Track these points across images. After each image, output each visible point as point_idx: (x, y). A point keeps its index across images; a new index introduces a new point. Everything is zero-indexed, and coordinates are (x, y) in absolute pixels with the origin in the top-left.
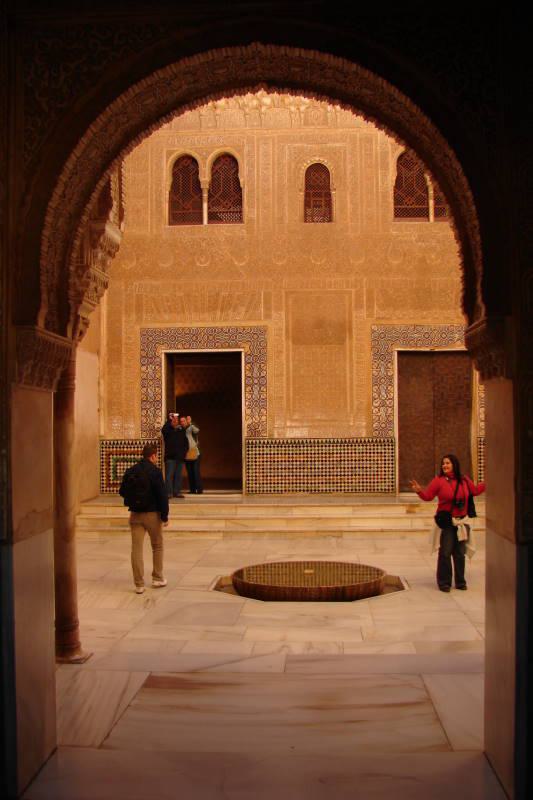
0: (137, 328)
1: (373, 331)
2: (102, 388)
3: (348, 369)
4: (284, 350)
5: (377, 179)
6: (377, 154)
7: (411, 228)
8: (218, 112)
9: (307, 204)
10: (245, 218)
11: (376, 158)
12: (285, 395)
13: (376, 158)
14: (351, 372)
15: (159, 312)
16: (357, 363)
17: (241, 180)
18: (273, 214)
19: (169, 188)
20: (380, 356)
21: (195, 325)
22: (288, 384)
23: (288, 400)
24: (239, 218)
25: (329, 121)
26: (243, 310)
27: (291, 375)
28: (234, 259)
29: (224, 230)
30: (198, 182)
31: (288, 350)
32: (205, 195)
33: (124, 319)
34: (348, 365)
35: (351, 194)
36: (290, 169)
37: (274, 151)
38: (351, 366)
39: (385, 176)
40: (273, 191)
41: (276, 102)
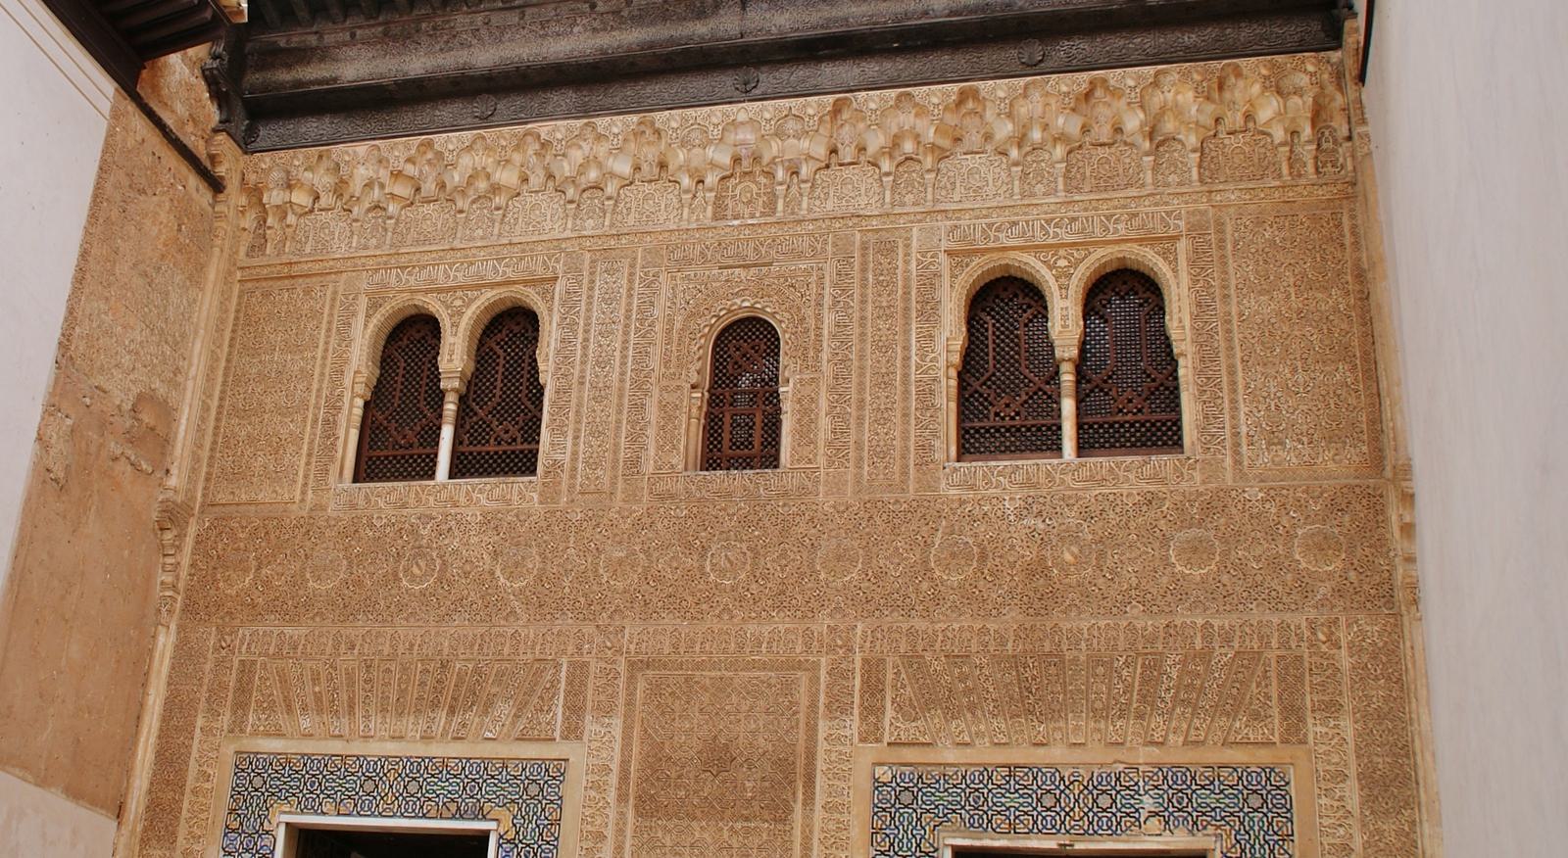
1: (878, 784)
5: (907, 348)
6: (907, 280)
11: (906, 293)
13: (906, 293)
17: (541, 367)
18: (616, 445)
19: (360, 389)
24: (524, 463)
25: (780, 206)
28: (498, 573)
29: (485, 492)
30: (436, 377)
32: (450, 407)
35: (832, 389)
36: (669, 331)
37: (630, 289)
40: (621, 389)
41: (645, 167)
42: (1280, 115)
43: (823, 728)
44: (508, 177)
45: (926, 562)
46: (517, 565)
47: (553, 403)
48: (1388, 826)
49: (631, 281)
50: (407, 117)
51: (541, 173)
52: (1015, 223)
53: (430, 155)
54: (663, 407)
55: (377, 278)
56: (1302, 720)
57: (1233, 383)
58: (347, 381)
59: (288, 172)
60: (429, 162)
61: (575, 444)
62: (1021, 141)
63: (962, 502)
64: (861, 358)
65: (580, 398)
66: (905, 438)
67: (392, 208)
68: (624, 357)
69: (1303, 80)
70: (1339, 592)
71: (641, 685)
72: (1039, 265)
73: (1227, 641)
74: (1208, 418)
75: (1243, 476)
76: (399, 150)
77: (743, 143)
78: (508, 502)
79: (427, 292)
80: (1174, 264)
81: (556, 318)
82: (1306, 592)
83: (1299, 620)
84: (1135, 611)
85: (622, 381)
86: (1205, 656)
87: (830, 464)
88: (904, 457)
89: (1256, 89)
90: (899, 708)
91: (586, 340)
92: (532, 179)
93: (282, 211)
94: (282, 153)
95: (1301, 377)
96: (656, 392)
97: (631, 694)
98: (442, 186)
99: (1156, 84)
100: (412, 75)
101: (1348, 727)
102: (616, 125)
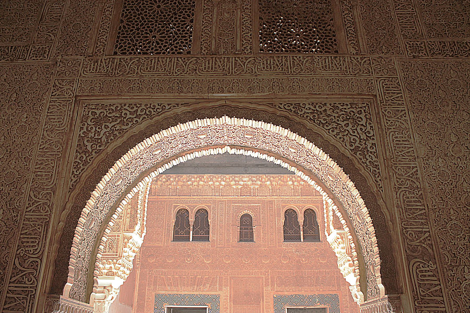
0: (154, 293)
4: (229, 307)
6: (275, 210)
21: (183, 293)
24: (207, 239)
26: (208, 285)
29: (200, 245)
31: (230, 307)
33: (147, 288)
52: (293, 200)
68: (225, 220)
91: (218, 216)
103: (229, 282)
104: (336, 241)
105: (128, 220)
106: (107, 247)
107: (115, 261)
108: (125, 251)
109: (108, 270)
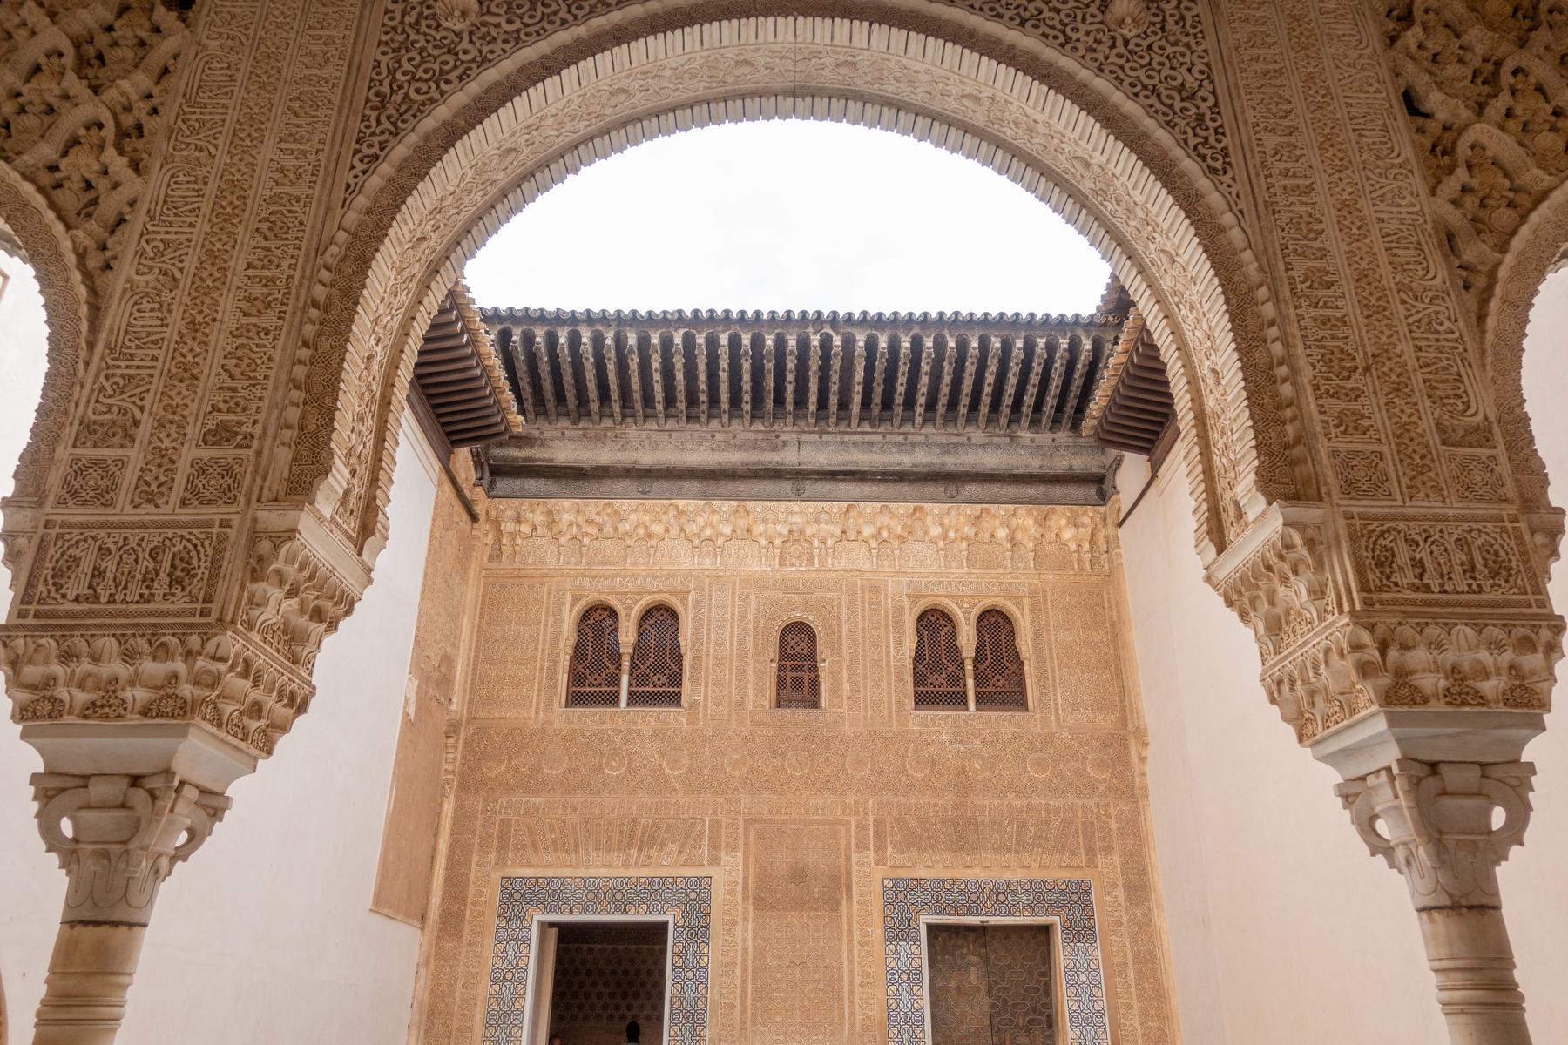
0: (496, 876)
2: (422, 982)
3: (845, 955)
4: (739, 919)
5: (888, 647)
6: (886, 608)
7: (941, 719)
8: (653, 542)
9: (781, 682)
10: (684, 700)
12: (738, 1002)
13: (887, 616)
14: (851, 961)
15: (535, 848)
16: (861, 944)
17: (683, 643)
18: (730, 692)
19: (570, 651)
20: (898, 931)
22: (744, 981)
23: (744, 1011)
24: (674, 699)
25: (816, 562)
26: (673, 848)
27: (750, 965)
29: (653, 716)
31: (745, 919)
32: (626, 664)
33: (475, 858)
34: (845, 948)
35: (849, 667)
36: (756, 628)
38: (850, 951)
39: (900, 642)
40: (731, 660)
41: (739, 531)
42: (1075, 537)
43: (855, 858)
44: (657, 529)
45: (904, 766)
46: (676, 761)
47: (692, 666)
48: (1138, 911)
49: (733, 597)
50: (593, 487)
51: (678, 529)
52: (941, 582)
53: (609, 511)
54: (756, 671)
55: (577, 582)
56: (1095, 855)
57: (1054, 677)
58: (561, 646)
59: (519, 514)
60: (608, 515)
61: (706, 691)
62: (945, 537)
63: (921, 734)
64: (864, 650)
65: (707, 664)
66: (890, 697)
67: (586, 541)
68: (732, 641)
69: (1086, 520)
70: (1109, 789)
71: (752, 834)
72: (954, 606)
73: (1057, 813)
74: (1043, 695)
75: (1061, 727)
76: (592, 507)
77: (795, 523)
78: (669, 724)
79: (609, 594)
80: (1022, 610)
81: (690, 616)
82: (1094, 789)
83: (1091, 803)
84: (1011, 795)
85: (731, 655)
86: (1047, 821)
87: (850, 709)
88: (889, 707)
89: (1063, 522)
90: (894, 847)
91: (709, 629)
92: (672, 531)
93: (513, 536)
94: (514, 500)
95: (1086, 676)
96: (751, 662)
97: (746, 837)
98: (616, 529)
99: (1014, 515)
100: (602, 463)
101: (1117, 860)
102: (726, 506)
103: (742, 838)
104: (1274, 560)
105: (284, 455)
106: (163, 576)
107: (194, 641)
108: (256, 600)
109: (157, 688)
